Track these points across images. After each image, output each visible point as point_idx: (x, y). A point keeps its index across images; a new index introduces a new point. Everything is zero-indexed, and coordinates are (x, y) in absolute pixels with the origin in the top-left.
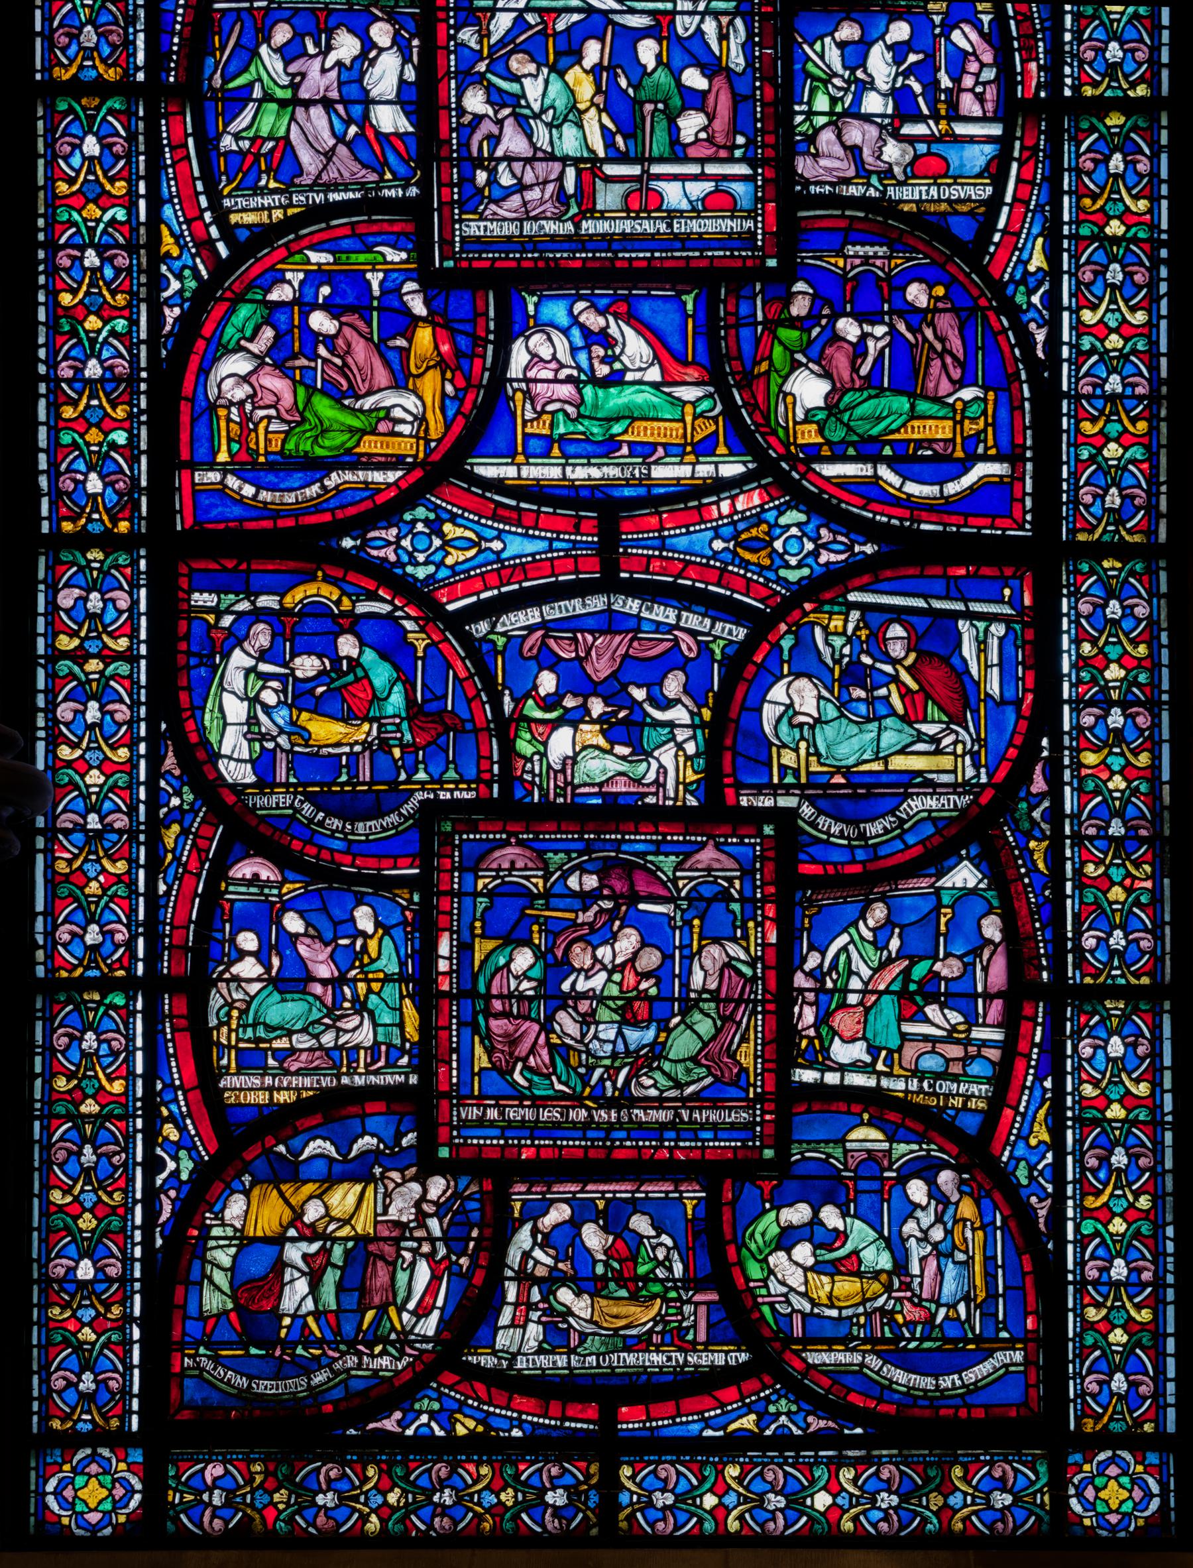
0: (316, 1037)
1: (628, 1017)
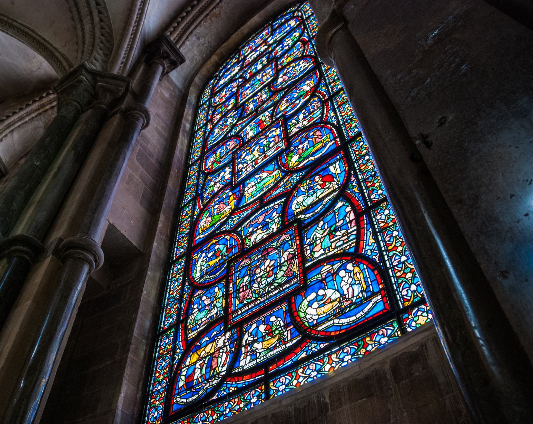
0: (206, 317)
1: (268, 276)
